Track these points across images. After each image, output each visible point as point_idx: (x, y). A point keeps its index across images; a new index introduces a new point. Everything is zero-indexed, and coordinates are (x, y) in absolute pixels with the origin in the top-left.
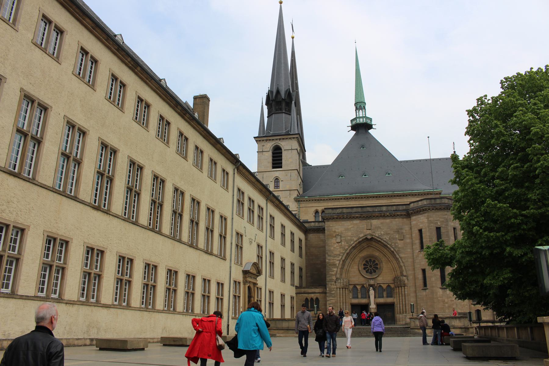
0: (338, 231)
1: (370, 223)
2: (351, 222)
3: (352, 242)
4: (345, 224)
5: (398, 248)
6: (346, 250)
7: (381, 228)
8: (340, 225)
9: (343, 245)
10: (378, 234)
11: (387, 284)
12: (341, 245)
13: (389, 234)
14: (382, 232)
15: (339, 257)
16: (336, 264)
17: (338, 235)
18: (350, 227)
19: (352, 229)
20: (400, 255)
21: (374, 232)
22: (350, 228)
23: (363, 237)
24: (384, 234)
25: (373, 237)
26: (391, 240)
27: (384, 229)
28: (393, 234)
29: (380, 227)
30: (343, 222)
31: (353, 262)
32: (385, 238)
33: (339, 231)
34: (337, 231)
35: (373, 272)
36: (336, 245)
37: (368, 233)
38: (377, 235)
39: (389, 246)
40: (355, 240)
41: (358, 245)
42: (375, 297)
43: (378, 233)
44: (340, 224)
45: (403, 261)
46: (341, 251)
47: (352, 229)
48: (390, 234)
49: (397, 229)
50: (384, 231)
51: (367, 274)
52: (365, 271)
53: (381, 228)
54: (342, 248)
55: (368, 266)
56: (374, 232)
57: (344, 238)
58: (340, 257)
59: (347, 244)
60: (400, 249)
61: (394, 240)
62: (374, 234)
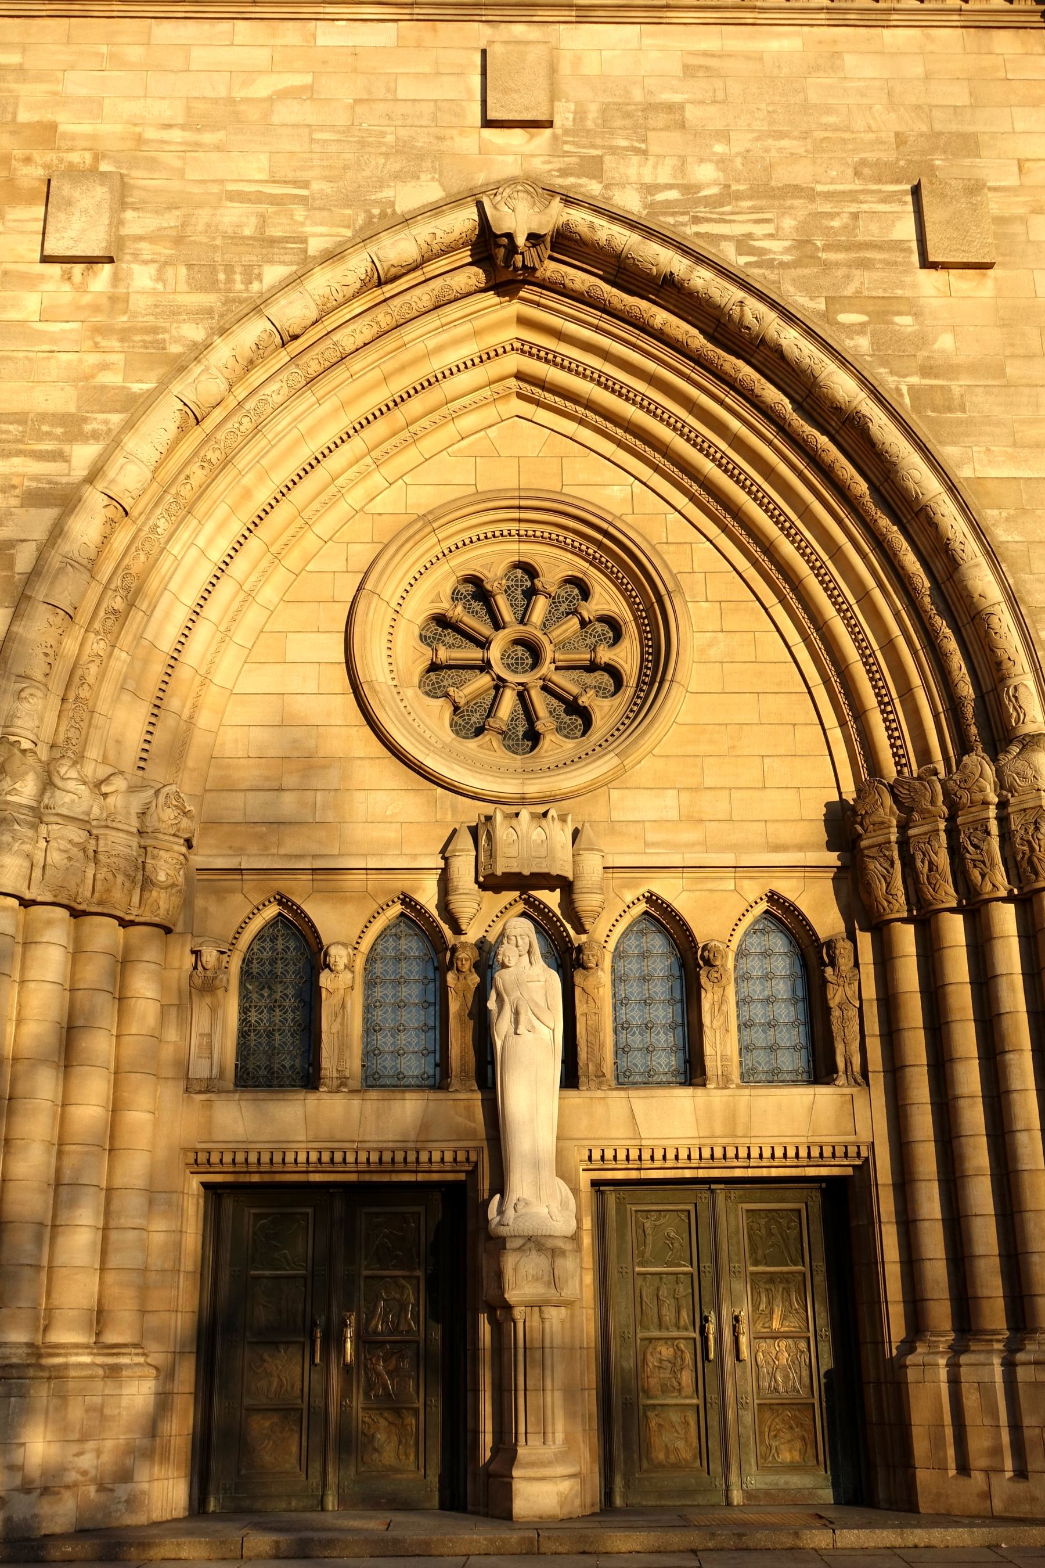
0: (86, 128)
1: (535, 55)
2: (291, 34)
3: (273, 274)
4: (200, 57)
5: (926, 371)
6: (179, 367)
7: (682, 126)
8: (117, 62)
9: (139, 303)
10: (651, 189)
11: (754, 889)
12: (117, 301)
13: (795, 190)
14: (705, 173)
15: (58, 456)
16: (11, 544)
17: (77, 175)
18: (263, 88)
19: (287, 113)
20: (948, 453)
21: (593, 168)
22: (270, 99)
23: (435, 209)
24: (727, 195)
25: (580, 219)
26: (827, 266)
27: (724, 136)
28: (852, 196)
29: (670, 108)
30: (166, 32)
31: (280, 576)
32: (743, 244)
33: (104, 128)
34: (69, 124)
35: (545, 722)
36: (30, 304)
37: (508, 167)
38: (630, 202)
39: (790, 339)
40: (315, 246)
41: (363, 331)
42: (570, 1078)
43: (634, 169)
44: (134, 53)
45: (1002, 534)
46: (111, 379)
47: (287, 113)
48: (811, 195)
49: (900, 139)
50: (721, 162)
51: (472, 744)
52: (438, 712)
53: (682, 126)
54: (124, 335)
55: (484, 644)
56: (593, 168)
57: (170, 220)
58: (83, 454)
59: (211, 286)
60: (957, 386)
61: (865, 264)
62: (593, 188)
